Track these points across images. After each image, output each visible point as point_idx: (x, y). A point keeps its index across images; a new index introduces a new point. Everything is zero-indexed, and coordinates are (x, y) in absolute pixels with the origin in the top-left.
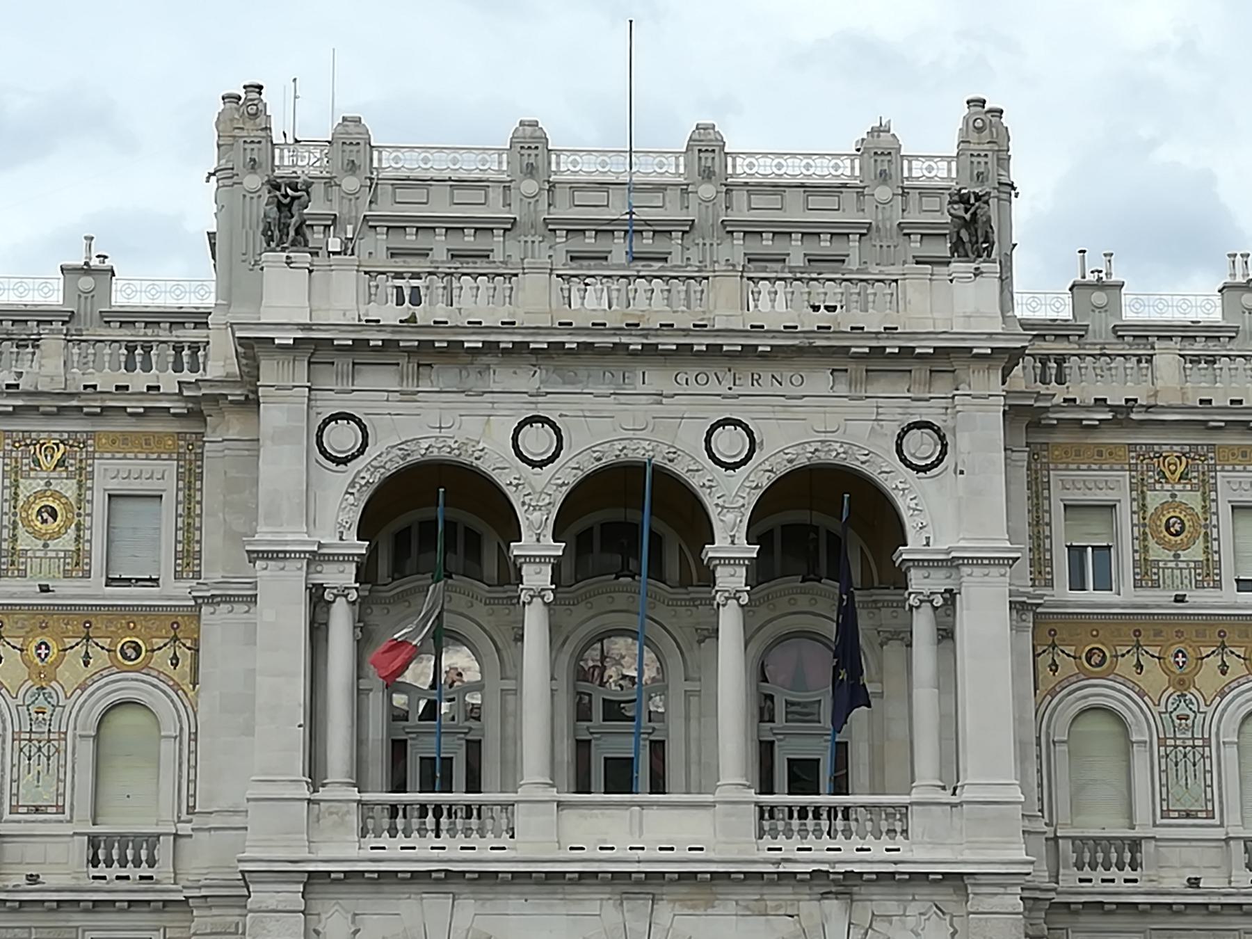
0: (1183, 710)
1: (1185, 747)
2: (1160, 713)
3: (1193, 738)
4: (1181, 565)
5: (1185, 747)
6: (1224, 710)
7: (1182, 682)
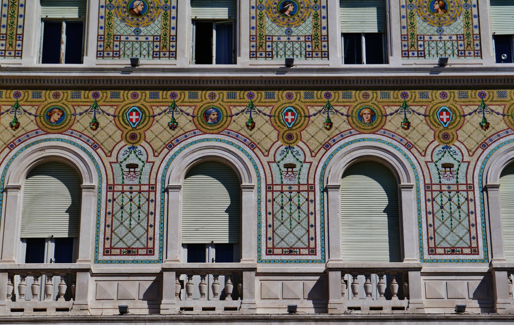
0: (133, 159)
1: (131, 192)
2: (111, 163)
3: (140, 185)
4: (141, 39)
5: (131, 192)
6: (172, 159)
7: (133, 137)
